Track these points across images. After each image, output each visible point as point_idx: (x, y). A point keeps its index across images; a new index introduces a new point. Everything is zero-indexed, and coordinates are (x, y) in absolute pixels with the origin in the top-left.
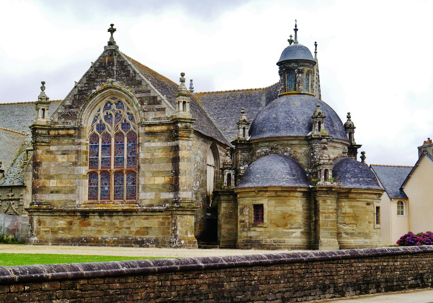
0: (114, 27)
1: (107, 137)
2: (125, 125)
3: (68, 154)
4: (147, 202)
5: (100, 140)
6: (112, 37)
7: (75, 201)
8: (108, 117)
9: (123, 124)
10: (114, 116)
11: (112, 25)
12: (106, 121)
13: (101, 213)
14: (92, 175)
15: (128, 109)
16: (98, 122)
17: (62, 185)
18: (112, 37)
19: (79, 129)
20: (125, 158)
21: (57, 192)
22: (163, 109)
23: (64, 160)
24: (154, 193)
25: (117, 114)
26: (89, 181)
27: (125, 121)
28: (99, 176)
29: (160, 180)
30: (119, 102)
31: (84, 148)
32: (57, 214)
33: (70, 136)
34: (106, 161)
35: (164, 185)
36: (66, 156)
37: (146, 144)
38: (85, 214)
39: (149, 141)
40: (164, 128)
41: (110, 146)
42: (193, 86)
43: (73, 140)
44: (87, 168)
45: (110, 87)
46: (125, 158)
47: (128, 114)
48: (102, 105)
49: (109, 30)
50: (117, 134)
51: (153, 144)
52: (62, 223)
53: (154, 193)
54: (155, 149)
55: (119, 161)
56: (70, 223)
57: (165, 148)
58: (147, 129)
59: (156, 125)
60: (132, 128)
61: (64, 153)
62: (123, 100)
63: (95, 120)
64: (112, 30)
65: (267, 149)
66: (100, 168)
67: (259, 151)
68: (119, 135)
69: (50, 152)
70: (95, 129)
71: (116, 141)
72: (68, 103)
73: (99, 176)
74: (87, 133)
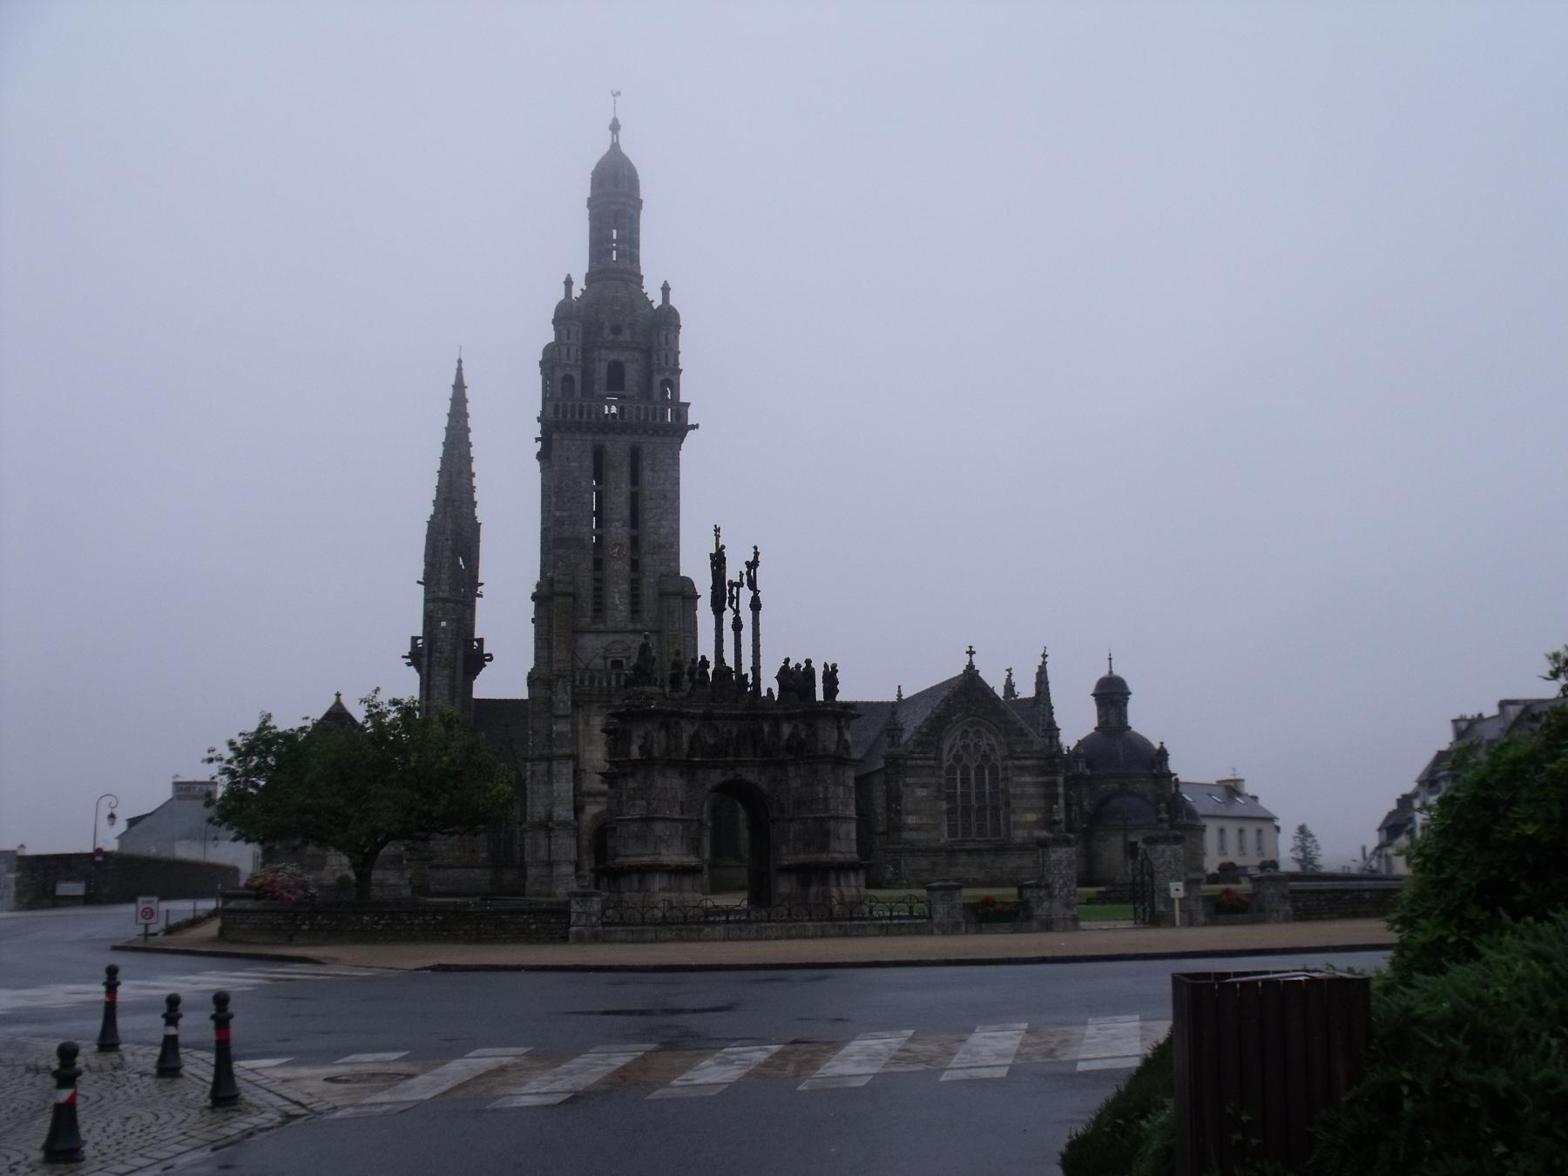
0: (973, 650)
1: (966, 769)
2: (986, 757)
3: (927, 787)
4: (1019, 840)
5: (958, 772)
6: (971, 660)
7: (939, 840)
8: (965, 747)
9: (982, 756)
10: (972, 746)
11: (971, 647)
12: (963, 751)
13: (970, 852)
14: (951, 811)
15: (988, 739)
16: (954, 752)
17: (921, 822)
18: (971, 660)
19: (938, 759)
20: (987, 792)
21: (917, 830)
22: (1032, 742)
23: (924, 794)
24: (1026, 831)
25: (975, 745)
26: (948, 817)
27: (985, 752)
28: (959, 812)
29: (1031, 817)
30: (978, 731)
31: (943, 781)
32: (920, 853)
33: (930, 767)
34: (965, 796)
35: (1036, 823)
36: (925, 790)
37: (1016, 779)
38: (951, 853)
39: (1018, 776)
40: (1033, 762)
41: (969, 779)
42: (902, 693)
43: (934, 773)
44: (945, 802)
45: (973, 715)
46: (987, 792)
47: (988, 744)
48: (958, 734)
49: (967, 652)
50: (978, 767)
51: (1023, 779)
52: (925, 863)
53: (1026, 831)
54: (1024, 784)
55: (980, 796)
56: (934, 864)
57: (1036, 784)
58: (1016, 762)
59: (1026, 758)
60: (992, 758)
61: (923, 786)
62: (983, 730)
63: (951, 750)
64: (971, 653)
65: (1116, 786)
66: (959, 802)
67: (1103, 786)
68: (980, 769)
69: (908, 785)
70: (951, 761)
71: (976, 774)
72: (924, 730)
73: (959, 812)
74: (945, 765)
